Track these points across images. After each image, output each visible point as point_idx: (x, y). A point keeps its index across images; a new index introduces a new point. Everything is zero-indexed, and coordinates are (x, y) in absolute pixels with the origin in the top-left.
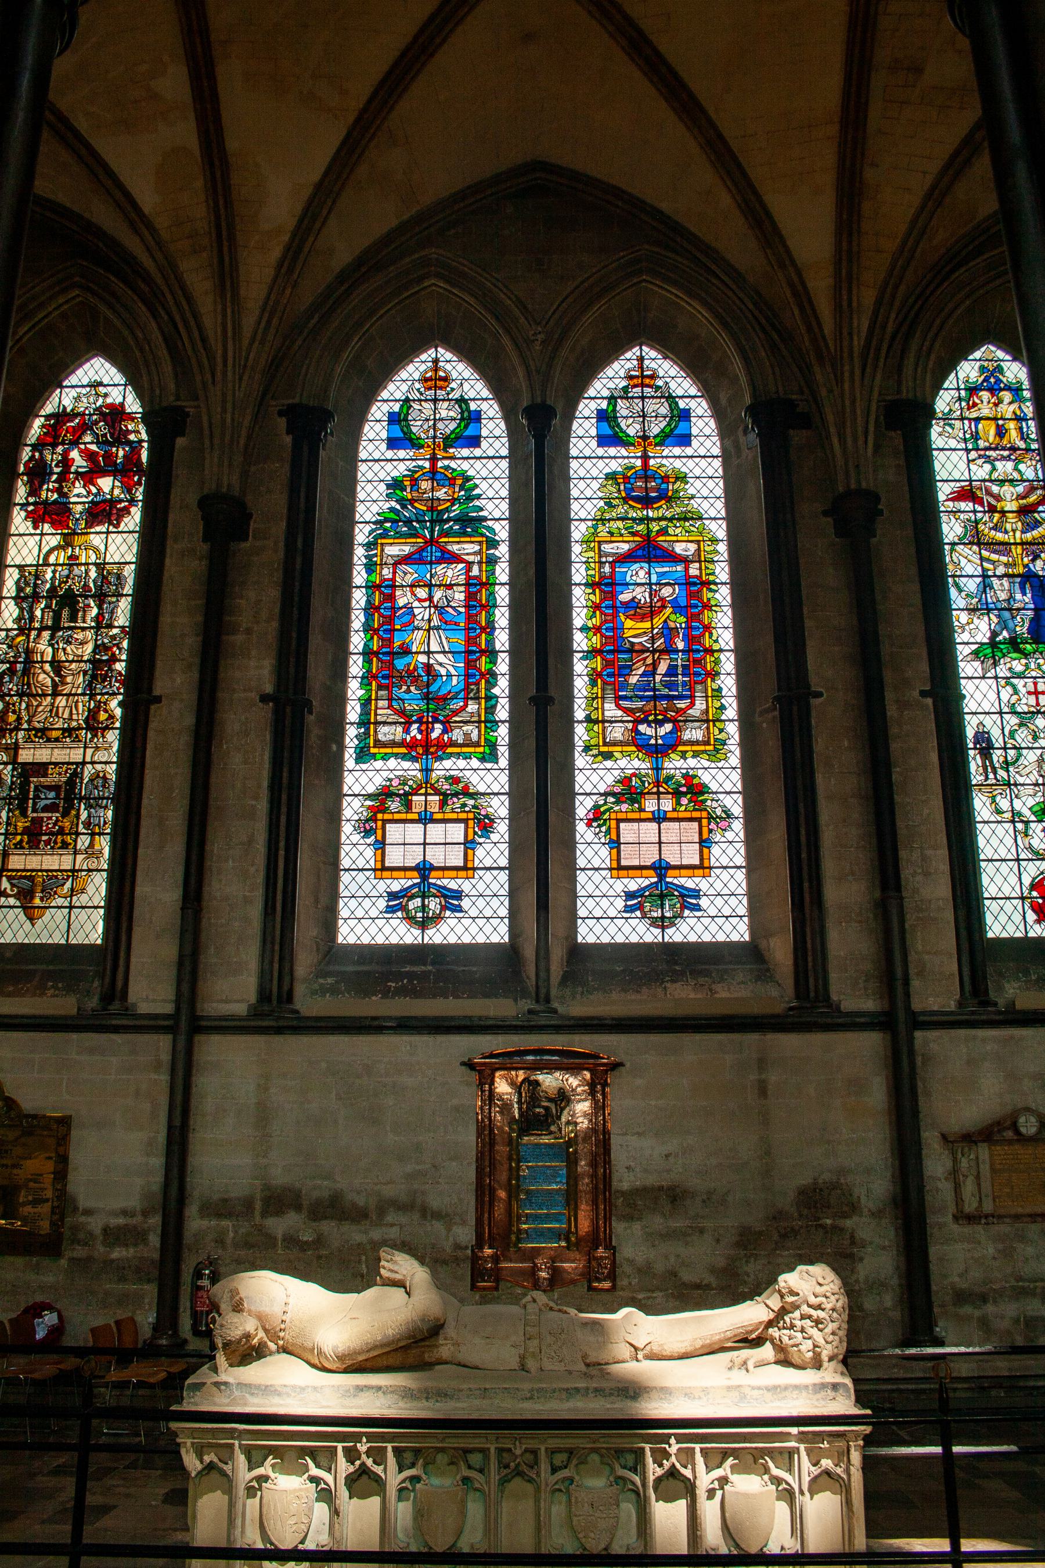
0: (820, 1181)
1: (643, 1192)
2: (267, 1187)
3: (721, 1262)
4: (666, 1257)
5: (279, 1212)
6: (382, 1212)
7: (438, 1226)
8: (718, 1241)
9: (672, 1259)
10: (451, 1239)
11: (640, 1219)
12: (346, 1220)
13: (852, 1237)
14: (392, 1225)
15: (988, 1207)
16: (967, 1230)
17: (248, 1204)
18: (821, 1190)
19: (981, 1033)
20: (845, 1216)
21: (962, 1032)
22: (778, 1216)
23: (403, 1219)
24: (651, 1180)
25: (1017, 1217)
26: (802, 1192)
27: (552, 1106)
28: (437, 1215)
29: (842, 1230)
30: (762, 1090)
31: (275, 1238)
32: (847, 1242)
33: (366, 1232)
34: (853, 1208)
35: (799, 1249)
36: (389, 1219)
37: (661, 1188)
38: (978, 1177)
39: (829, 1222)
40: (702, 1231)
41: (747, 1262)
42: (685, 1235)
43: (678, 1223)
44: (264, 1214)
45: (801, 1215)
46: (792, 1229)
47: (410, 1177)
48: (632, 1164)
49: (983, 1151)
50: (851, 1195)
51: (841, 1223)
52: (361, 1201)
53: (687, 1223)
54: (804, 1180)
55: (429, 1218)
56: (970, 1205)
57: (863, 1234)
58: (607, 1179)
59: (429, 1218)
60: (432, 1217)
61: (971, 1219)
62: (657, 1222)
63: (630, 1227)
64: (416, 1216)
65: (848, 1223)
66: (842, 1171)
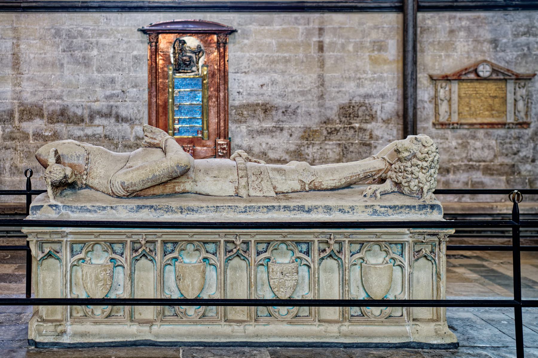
0: (353, 102)
1: (247, 106)
2: (21, 104)
3: (293, 148)
4: (260, 144)
5: (30, 119)
6: (91, 118)
7: (126, 126)
8: (291, 135)
9: (264, 145)
10: (134, 133)
11: (245, 122)
12: (71, 123)
13: (371, 134)
14: (99, 126)
15: (455, 118)
16: (441, 132)
17: (11, 114)
18: (353, 107)
19: (459, 14)
20: (367, 122)
21: (447, 14)
22: (327, 121)
23: (104, 122)
24: (253, 100)
25: (472, 125)
26: (342, 108)
27: (193, 56)
28: (125, 120)
29: (365, 130)
30: (321, 48)
31: (28, 134)
32: (367, 137)
33: (83, 130)
34: (373, 117)
35: (339, 140)
36: (97, 121)
37: (258, 105)
38: (450, 101)
39: (357, 125)
40: (282, 129)
41: (308, 147)
42: (272, 131)
43: (268, 124)
44: (21, 120)
45: (341, 121)
46: (335, 129)
47: (108, 98)
48: (241, 90)
49: (455, 86)
50: (371, 110)
51: (364, 126)
52: (79, 112)
53: (274, 124)
54: (344, 100)
55: (120, 121)
56: (443, 118)
57: (377, 133)
58: (226, 99)
59: (120, 121)
60: (122, 120)
61: (443, 125)
62: (255, 124)
63: (239, 127)
64: (113, 120)
65: (369, 126)
66: (367, 96)
